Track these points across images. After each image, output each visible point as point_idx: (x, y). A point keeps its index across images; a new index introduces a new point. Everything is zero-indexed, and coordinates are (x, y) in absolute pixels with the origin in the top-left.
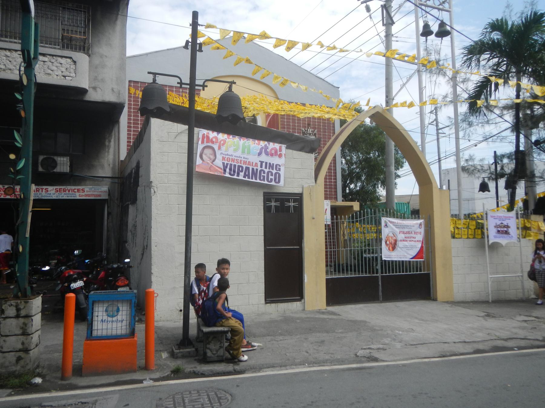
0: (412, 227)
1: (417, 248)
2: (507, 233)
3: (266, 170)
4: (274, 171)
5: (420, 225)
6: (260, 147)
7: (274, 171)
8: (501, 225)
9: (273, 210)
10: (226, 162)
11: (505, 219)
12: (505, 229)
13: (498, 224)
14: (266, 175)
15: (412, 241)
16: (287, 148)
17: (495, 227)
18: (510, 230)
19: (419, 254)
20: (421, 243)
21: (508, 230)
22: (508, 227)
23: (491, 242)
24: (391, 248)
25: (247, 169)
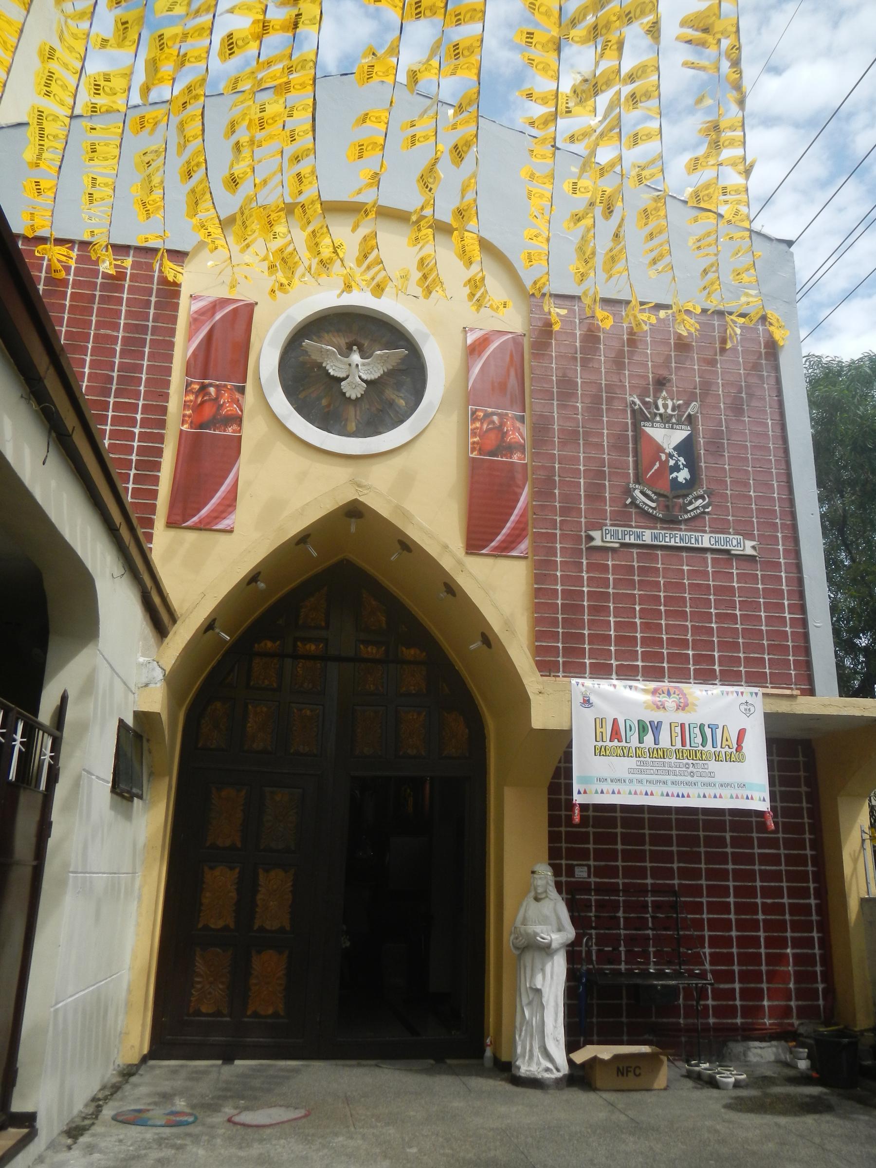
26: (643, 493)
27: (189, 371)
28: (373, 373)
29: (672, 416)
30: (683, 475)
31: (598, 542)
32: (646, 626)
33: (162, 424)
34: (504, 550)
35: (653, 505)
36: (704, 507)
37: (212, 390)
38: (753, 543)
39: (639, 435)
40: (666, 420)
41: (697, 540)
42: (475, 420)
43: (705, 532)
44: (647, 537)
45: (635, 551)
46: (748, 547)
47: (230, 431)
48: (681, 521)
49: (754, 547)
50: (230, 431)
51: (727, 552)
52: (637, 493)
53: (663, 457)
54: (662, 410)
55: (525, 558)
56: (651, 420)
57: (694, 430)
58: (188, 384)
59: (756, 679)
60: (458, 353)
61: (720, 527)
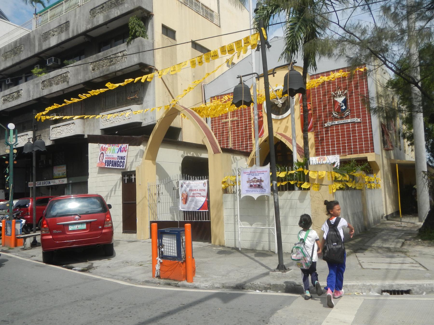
0: (198, 186)
2: (259, 186)
3: (120, 161)
4: (122, 161)
5: (204, 184)
6: (119, 148)
7: (122, 161)
8: (254, 180)
10: (106, 160)
12: (258, 183)
13: (250, 179)
14: (119, 163)
15: (198, 196)
16: (129, 145)
17: (248, 182)
18: (263, 184)
19: (202, 207)
23: (242, 196)
24: (184, 202)
25: (113, 161)
26: (335, 113)
28: (283, 102)
29: (341, 95)
30: (344, 108)
31: (326, 126)
32: (337, 141)
36: (349, 113)
40: (340, 96)
42: (301, 107)
44: (336, 122)
46: (359, 120)
47: (261, 119)
49: (360, 120)
50: (261, 119)
51: (354, 122)
52: (334, 114)
54: (339, 94)
55: (313, 131)
56: (337, 97)
57: (347, 96)
59: (339, 153)
61: (353, 117)
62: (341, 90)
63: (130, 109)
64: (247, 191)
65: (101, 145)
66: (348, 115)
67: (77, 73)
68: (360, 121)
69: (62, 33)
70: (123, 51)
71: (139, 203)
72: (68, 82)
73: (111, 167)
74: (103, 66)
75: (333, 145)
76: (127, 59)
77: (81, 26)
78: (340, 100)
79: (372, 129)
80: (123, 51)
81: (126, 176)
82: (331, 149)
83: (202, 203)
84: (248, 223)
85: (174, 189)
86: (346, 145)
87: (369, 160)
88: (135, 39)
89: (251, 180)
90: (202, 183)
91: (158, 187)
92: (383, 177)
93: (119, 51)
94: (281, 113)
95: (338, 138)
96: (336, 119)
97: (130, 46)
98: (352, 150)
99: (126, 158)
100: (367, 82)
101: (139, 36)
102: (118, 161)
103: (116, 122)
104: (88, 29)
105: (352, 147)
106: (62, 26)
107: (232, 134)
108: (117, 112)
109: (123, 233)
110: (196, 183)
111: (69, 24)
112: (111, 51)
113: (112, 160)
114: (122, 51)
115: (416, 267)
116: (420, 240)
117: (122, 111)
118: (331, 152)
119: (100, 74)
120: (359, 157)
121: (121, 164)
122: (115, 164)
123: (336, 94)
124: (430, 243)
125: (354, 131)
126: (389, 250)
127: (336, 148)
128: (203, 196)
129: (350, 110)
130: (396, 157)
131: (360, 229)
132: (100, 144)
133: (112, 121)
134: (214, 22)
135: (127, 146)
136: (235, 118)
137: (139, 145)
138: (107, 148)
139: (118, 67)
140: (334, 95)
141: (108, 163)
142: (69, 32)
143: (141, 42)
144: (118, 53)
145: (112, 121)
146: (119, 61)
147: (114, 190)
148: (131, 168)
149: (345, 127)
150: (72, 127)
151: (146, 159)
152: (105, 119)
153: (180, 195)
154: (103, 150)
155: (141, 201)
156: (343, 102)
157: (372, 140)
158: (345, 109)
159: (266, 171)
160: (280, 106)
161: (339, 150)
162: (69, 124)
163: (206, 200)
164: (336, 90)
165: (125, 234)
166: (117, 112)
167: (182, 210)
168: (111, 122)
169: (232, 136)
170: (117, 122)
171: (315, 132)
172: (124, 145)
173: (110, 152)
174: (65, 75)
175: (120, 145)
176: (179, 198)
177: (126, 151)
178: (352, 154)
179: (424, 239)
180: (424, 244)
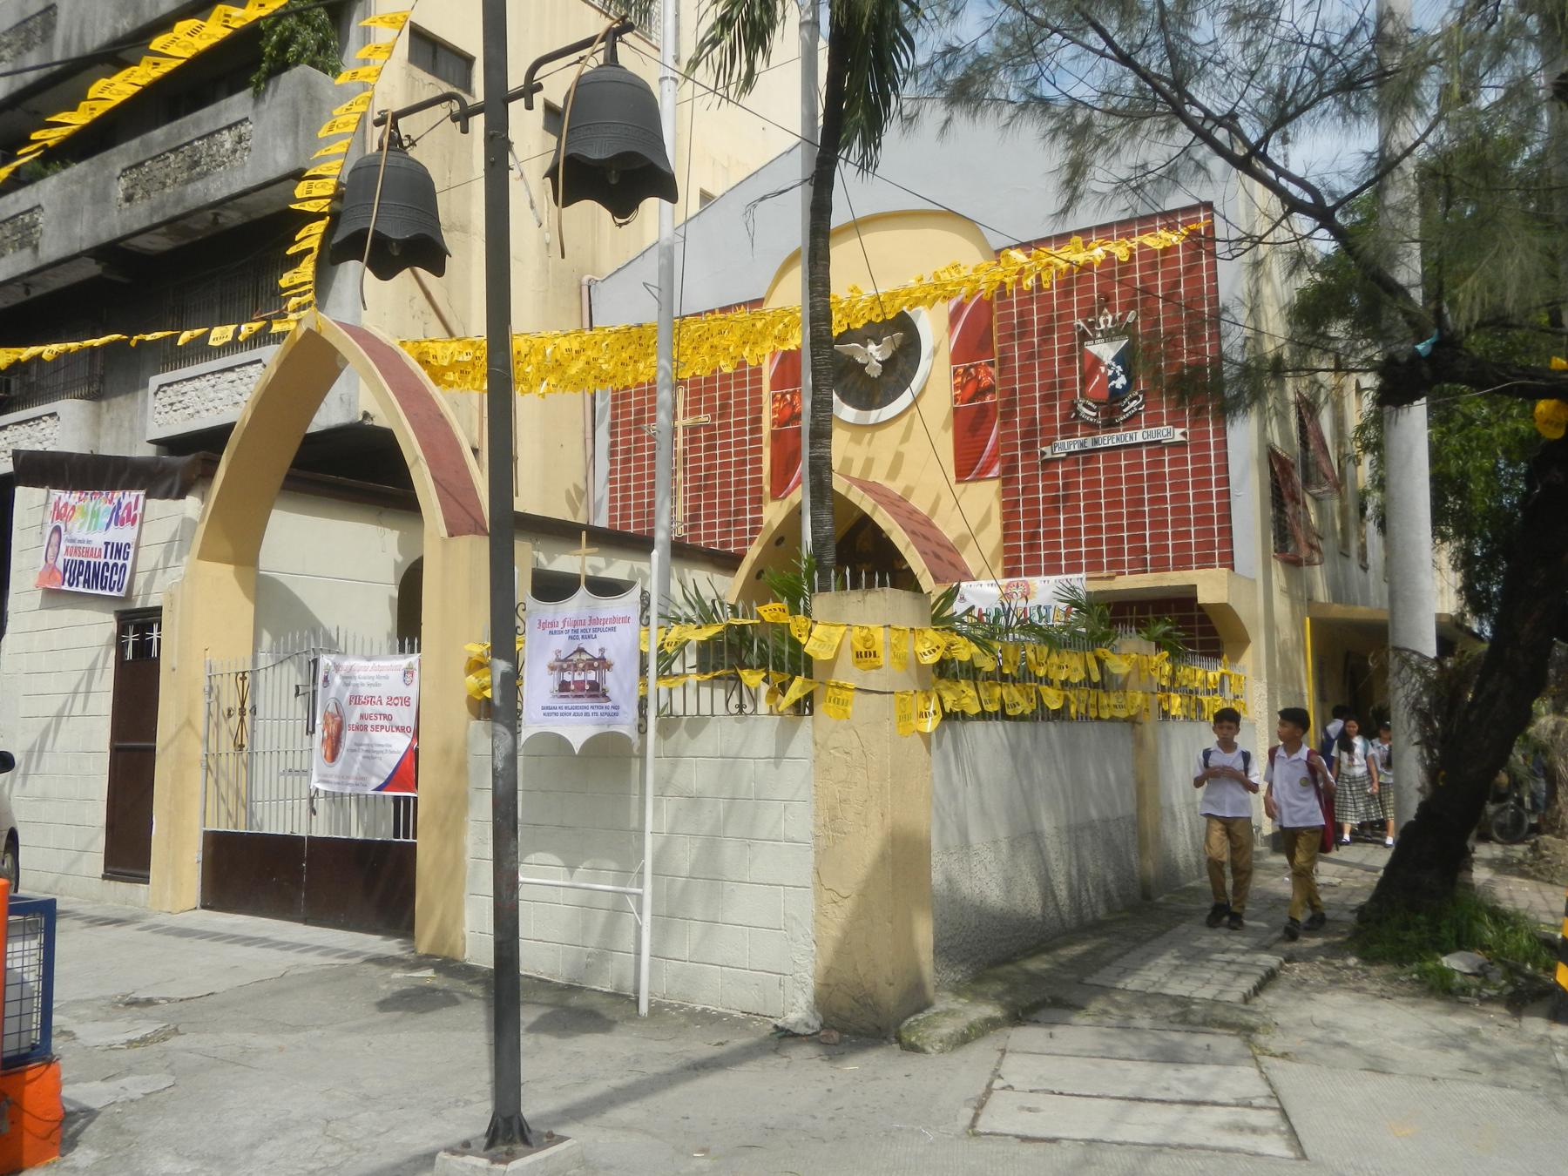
1: (392, 752)
2: (596, 691)
3: (111, 562)
4: (120, 562)
5: (408, 672)
6: (112, 507)
7: (120, 562)
8: (576, 658)
9: (129, 655)
10: (68, 558)
11: (595, 631)
12: (592, 676)
14: (108, 574)
16: (148, 496)
17: (552, 668)
18: (611, 682)
20: (411, 735)
21: (603, 679)
22: (602, 664)
25: (89, 563)
26: (1085, 405)
27: (774, 386)
28: (888, 354)
30: (1121, 382)
31: (1049, 456)
32: (1088, 519)
33: (759, 430)
34: (981, 477)
35: (1094, 414)
37: (788, 396)
38: (1182, 430)
39: (1084, 354)
41: (1131, 438)
43: (1140, 428)
45: (1081, 456)
46: (1178, 435)
48: (1118, 424)
49: (1184, 434)
51: (1159, 442)
52: (1080, 406)
53: (1103, 369)
54: (1103, 327)
56: (1094, 339)
58: (774, 396)
60: (946, 320)
61: (1155, 421)
62: (1113, 311)
63: (259, 361)
64: (548, 711)
65: (57, 494)
66: (1136, 415)
67: (70, 213)
68: (1183, 439)
69: (29, 49)
70: (240, 122)
71: (164, 750)
72: (36, 248)
73: (80, 589)
74: (164, 185)
75: (1073, 533)
76: (252, 154)
77: (98, 23)
78: (1105, 351)
79: (1227, 472)
80: (240, 122)
81: (131, 629)
82: (1063, 551)
83: (394, 760)
84: (558, 861)
85: (297, 694)
86: (1125, 535)
87: (1205, 597)
88: (285, 75)
89: (566, 660)
90: (397, 668)
91: (240, 683)
92: (1264, 673)
93: (224, 123)
94: (878, 400)
95: (1093, 507)
96: (1091, 428)
97: (263, 107)
98: (1148, 557)
99: (131, 551)
100: (1216, 280)
101: (296, 63)
102: (106, 564)
103: (204, 414)
104: (120, 34)
105: (1148, 544)
106: (31, 24)
107: (685, 483)
108: (213, 373)
109: (104, 877)
110: (381, 669)
111: (55, 14)
112: (197, 124)
113: (85, 561)
114: (236, 124)
115: (1254, 1130)
116: (1352, 961)
117: (231, 369)
118: (1063, 562)
119: (151, 215)
120: (1165, 584)
121: (115, 578)
122: (96, 575)
123: (1091, 325)
124: (1392, 979)
125: (1158, 478)
126: (1185, 1014)
127: (1083, 549)
128: (402, 729)
129: (1145, 393)
130: (1339, 591)
131: (1115, 894)
132: (52, 491)
133: (191, 411)
134: (654, 42)
135: (141, 498)
136: (704, 418)
137: (181, 495)
138: (73, 508)
139: (219, 189)
140: (1084, 331)
141: (75, 570)
142: (51, 47)
143: (309, 86)
144: (219, 131)
145: (191, 411)
146: (224, 163)
147: (82, 688)
148: (147, 594)
149: (1123, 463)
150: (47, 431)
151: (203, 555)
152: (166, 401)
153: (318, 722)
154: (59, 516)
155: (172, 741)
156: (1117, 359)
157: (1226, 517)
158: (1126, 388)
159: (626, 620)
160: (874, 370)
161: (1094, 555)
162: (40, 418)
163: (410, 746)
164: (1091, 312)
165: (112, 883)
166: (213, 373)
167: (321, 787)
168: (187, 411)
169: (685, 489)
170: (210, 413)
171: (1005, 482)
172: (130, 497)
173: (82, 525)
174: (27, 218)
175: (118, 494)
176: (314, 731)
177: (133, 524)
178: (1145, 572)
179: (1369, 959)
180: (1366, 983)
